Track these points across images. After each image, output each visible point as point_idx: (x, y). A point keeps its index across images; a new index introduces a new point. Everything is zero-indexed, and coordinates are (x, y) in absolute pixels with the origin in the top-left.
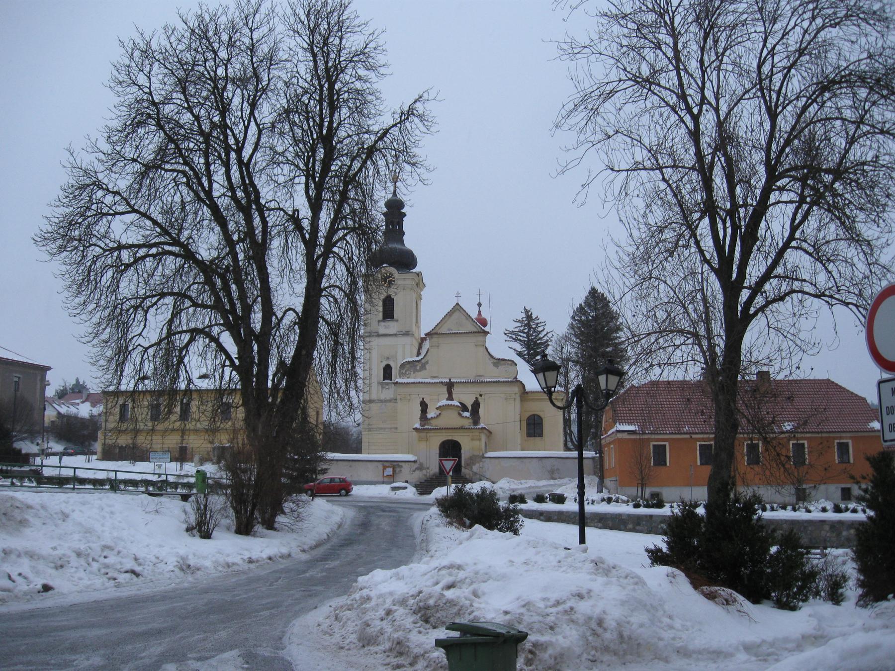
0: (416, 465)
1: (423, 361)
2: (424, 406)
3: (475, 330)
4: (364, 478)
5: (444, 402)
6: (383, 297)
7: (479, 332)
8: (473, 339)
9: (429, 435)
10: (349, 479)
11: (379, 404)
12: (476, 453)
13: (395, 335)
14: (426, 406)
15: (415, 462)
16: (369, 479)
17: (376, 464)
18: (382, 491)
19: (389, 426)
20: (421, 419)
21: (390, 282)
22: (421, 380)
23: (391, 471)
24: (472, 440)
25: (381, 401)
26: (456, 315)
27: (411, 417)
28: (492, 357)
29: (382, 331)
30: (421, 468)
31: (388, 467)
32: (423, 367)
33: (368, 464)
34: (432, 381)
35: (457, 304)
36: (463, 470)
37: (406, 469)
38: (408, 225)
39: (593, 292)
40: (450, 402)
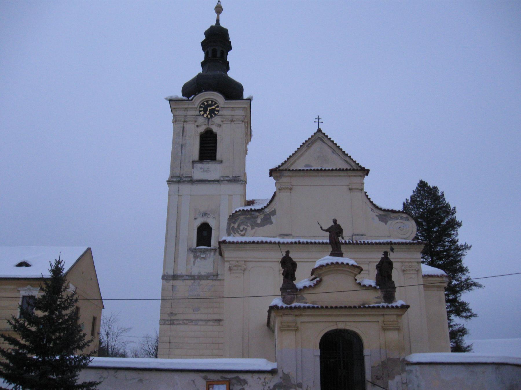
0: (276, 380)
1: (267, 210)
2: (289, 267)
3: (349, 168)
5: (327, 259)
6: (202, 129)
8: (344, 181)
9: (300, 319)
11: (190, 282)
12: (395, 355)
13: (218, 181)
14: (294, 265)
15: (273, 372)
17: (192, 376)
19: (204, 317)
21: (212, 112)
22: (264, 239)
25: (192, 278)
26: (318, 146)
28: (377, 207)
31: (218, 383)
32: (267, 221)
33: (176, 376)
34: (282, 240)
35: (319, 130)
38: (231, 57)
39: (422, 185)
40: (340, 260)
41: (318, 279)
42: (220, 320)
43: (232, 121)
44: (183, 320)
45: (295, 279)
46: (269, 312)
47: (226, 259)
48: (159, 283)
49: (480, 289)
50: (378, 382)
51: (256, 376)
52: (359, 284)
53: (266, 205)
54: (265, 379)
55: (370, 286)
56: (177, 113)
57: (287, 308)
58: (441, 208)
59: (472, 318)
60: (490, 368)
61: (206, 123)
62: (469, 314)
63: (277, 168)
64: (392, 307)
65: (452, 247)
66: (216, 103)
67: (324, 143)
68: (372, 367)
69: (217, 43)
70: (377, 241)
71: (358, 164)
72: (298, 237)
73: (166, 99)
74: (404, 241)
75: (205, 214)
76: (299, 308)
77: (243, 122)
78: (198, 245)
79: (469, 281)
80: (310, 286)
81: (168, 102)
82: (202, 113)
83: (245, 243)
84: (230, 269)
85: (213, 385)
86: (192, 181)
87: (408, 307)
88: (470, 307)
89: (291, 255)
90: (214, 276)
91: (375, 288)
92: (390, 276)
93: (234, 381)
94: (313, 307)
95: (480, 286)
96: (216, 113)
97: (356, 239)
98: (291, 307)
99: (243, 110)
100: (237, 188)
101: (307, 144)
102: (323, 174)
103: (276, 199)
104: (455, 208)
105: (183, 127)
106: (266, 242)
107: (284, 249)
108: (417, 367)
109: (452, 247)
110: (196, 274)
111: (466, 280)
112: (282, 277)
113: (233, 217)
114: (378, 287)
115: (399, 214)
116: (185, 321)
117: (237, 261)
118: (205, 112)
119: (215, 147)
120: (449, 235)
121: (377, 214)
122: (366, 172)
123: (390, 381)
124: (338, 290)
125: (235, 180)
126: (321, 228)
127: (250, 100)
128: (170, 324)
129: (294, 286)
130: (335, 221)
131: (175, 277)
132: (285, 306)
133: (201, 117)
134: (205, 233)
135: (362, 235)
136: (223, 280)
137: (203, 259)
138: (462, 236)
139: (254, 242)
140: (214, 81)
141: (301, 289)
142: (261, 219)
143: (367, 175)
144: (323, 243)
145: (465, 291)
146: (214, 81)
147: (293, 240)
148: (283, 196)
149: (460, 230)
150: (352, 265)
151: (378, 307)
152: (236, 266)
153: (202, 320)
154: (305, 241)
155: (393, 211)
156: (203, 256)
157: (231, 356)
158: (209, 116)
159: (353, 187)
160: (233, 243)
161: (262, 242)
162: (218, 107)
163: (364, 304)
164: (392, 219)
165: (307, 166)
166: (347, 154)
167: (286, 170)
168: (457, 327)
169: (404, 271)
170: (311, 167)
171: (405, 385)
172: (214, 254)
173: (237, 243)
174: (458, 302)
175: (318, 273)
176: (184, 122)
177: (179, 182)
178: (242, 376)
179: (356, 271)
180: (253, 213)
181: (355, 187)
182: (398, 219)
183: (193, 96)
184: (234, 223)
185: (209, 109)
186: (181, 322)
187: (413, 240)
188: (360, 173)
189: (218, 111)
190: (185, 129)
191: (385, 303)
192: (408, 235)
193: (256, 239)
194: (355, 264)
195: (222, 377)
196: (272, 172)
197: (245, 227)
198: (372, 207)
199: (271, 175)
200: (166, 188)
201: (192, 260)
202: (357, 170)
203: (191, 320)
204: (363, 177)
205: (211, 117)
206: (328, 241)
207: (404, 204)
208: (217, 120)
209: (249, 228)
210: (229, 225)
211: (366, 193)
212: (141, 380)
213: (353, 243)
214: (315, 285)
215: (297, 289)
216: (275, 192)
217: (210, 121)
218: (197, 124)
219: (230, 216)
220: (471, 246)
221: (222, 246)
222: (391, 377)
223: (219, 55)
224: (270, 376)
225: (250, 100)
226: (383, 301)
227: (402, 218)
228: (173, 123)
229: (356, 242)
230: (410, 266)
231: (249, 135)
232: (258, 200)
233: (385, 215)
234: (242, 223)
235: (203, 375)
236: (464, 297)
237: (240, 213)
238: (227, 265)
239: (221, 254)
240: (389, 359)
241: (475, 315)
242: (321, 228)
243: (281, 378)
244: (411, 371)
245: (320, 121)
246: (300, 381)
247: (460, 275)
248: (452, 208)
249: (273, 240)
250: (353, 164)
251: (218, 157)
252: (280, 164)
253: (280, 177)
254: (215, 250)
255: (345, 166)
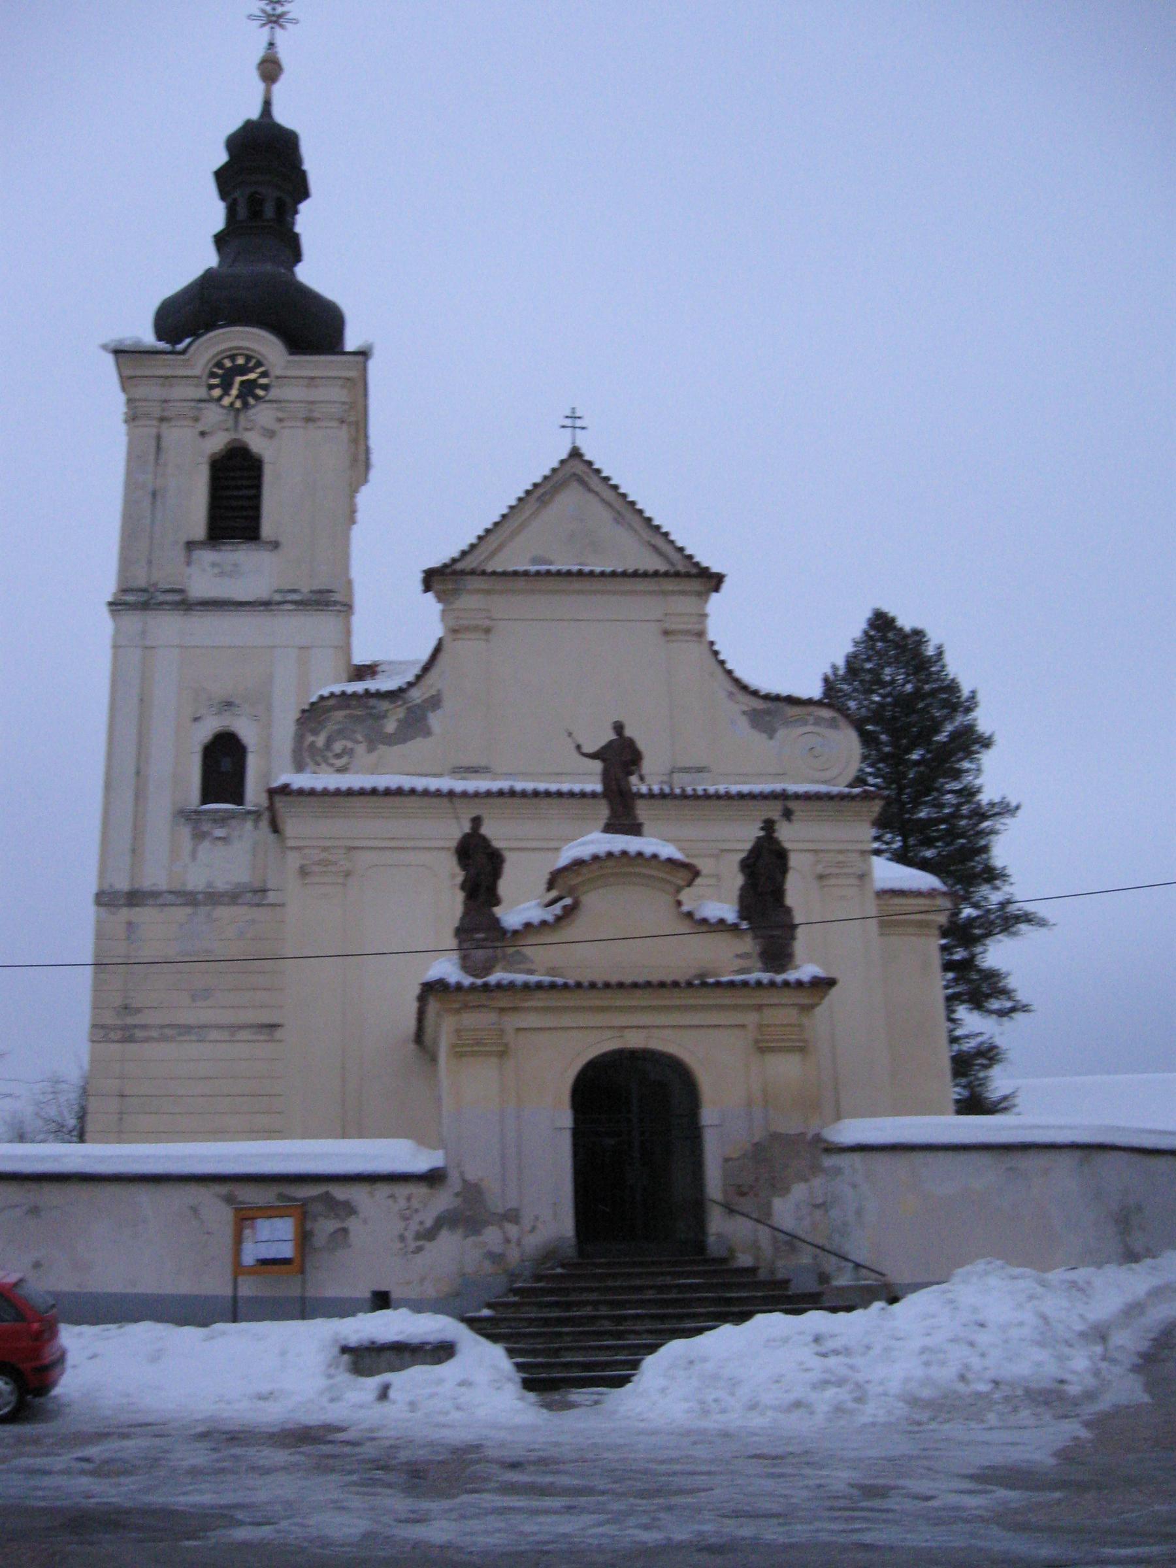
0: (443, 1200)
1: (416, 695)
2: (480, 865)
3: (662, 567)
4: (110, 1276)
5: (596, 841)
6: (217, 443)
7: (677, 574)
9: (513, 1021)
10: (41, 1287)
12: (790, 1125)
13: (266, 604)
15: (433, 1178)
16: (149, 1283)
18: (277, 1368)
19: (227, 1017)
20: (462, 932)
21: (249, 388)
22: (407, 782)
23: (281, 1246)
24: (762, 1049)
25: (190, 899)
26: (570, 499)
27: (411, 923)
28: (744, 688)
29: (202, 585)
30: (470, 1215)
31: (270, 1212)
32: (415, 724)
33: (144, 1196)
34: (459, 785)
35: (575, 454)
36: (718, 1224)
37: (376, 1220)
38: (308, 221)
39: (881, 623)
40: (632, 844)
41: (568, 901)
42: (273, 1026)
43: (309, 420)
44: (162, 1027)
45: (497, 901)
46: (422, 999)
47: (291, 843)
48: (89, 912)
49: (1044, 930)
50: (745, 1204)
51: (383, 1190)
52: (690, 915)
53: (410, 678)
54: (409, 1199)
55: (722, 921)
56: (141, 391)
57: (473, 988)
58: (933, 693)
59: (1018, 1016)
60: (1066, 1161)
61: (230, 424)
62: (1009, 1004)
63: (445, 566)
64: (786, 984)
65: (965, 810)
66: (259, 364)
67: (590, 490)
68: (727, 1160)
69: (263, 174)
70: (745, 788)
71: (690, 557)
72: (508, 775)
73: (104, 347)
74: (823, 788)
75: (228, 705)
76: (511, 986)
77: (343, 422)
78: (205, 801)
79: (1012, 909)
80: (544, 923)
81: (110, 359)
82: (217, 392)
83: (350, 793)
84: (303, 872)
85: (253, 1218)
86: (186, 605)
87: (830, 983)
88: (1011, 982)
89: (485, 830)
90: (255, 892)
91: (734, 928)
92: (778, 893)
93: (318, 1208)
94: (553, 986)
95: (1042, 923)
96: (260, 393)
97: (682, 783)
98: (486, 986)
99: (343, 387)
100: (320, 625)
101: (541, 491)
102: (585, 584)
103: (443, 658)
104: (973, 693)
105: (159, 438)
106: (413, 792)
107: (468, 812)
108: (857, 1157)
109: (965, 810)
110: (200, 889)
111: (1003, 905)
112: (460, 896)
113: (313, 715)
114: (744, 925)
115: (811, 709)
116: (167, 1031)
117: (325, 849)
118: (226, 392)
119: (257, 497)
120: (957, 774)
121: (746, 708)
122: (715, 581)
123: (778, 1204)
124: (626, 935)
125: (318, 603)
126: (578, 747)
127: (364, 354)
128: (123, 1041)
129: (495, 922)
130: (619, 728)
131: (134, 898)
132: (467, 981)
133: (213, 406)
134: (226, 764)
135: (700, 770)
136: (282, 905)
137: (219, 843)
138: (992, 777)
139: (374, 792)
140: (255, 295)
141: (515, 932)
142: (399, 721)
143: (717, 589)
144: (583, 795)
145: (999, 937)
146: (255, 295)
147: (495, 786)
148: (466, 649)
149: (987, 758)
150: (670, 860)
151: (745, 984)
152: (319, 863)
153: (219, 1027)
154: (529, 786)
155: (791, 701)
156: (219, 832)
157: (305, 1135)
158: (238, 404)
159: (673, 627)
160: (312, 793)
161: (399, 792)
162: (264, 374)
163: (701, 976)
164: (788, 723)
165: (534, 561)
166: (657, 528)
167: (473, 572)
168: (972, 1043)
169: (821, 877)
170: (551, 563)
171: (818, 1213)
172: (256, 827)
173: (325, 793)
174: (980, 971)
175: (568, 883)
176: (162, 419)
177: (145, 606)
178: (340, 1192)
179: (680, 878)
180: (373, 702)
181: (681, 627)
182: (805, 723)
183: (188, 340)
184: (315, 732)
185: (239, 382)
186: (154, 1034)
187: (850, 786)
188: (696, 585)
189: (265, 387)
190: (164, 444)
191: (766, 970)
192: (834, 772)
193: (383, 781)
194: (678, 855)
195: (281, 1196)
196: (432, 579)
197: (349, 745)
198: (730, 686)
199: (427, 588)
200: (105, 625)
201: (186, 842)
202: (688, 575)
203: (184, 1026)
204: (703, 595)
205: (246, 405)
206: (599, 788)
207: (826, 680)
208: (262, 414)
209: (361, 749)
210: (299, 738)
211: (712, 643)
212: (35, 1211)
213: (671, 796)
214: (559, 919)
215: (503, 932)
216: (440, 641)
217: (242, 417)
218: (201, 427)
219: (304, 711)
220: (1017, 808)
221: (280, 802)
222: (780, 1187)
223: (269, 212)
224: (421, 1190)
225: (364, 354)
226: (759, 965)
227: (818, 721)
228: (126, 422)
229: (683, 790)
230: (840, 864)
231: (360, 464)
232: (390, 663)
233: (768, 712)
234: (341, 733)
235: (224, 1189)
236: (996, 954)
237: (332, 702)
238: (294, 861)
239: (275, 828)
240: (775, 1137)
241: (1025, 1008)
242: (578, 747)
243: (457, 1195)
244: (838, 1171)
245: (579, 423)
246: (513, 1204)
247: (985, 889)
248: (965, 692)
249: (433, 784)
250: (676, 557)
251: (267, 529)
252: (455, 553)
253: (456, 592)
254: (256, 815)
255: (653, 563)
